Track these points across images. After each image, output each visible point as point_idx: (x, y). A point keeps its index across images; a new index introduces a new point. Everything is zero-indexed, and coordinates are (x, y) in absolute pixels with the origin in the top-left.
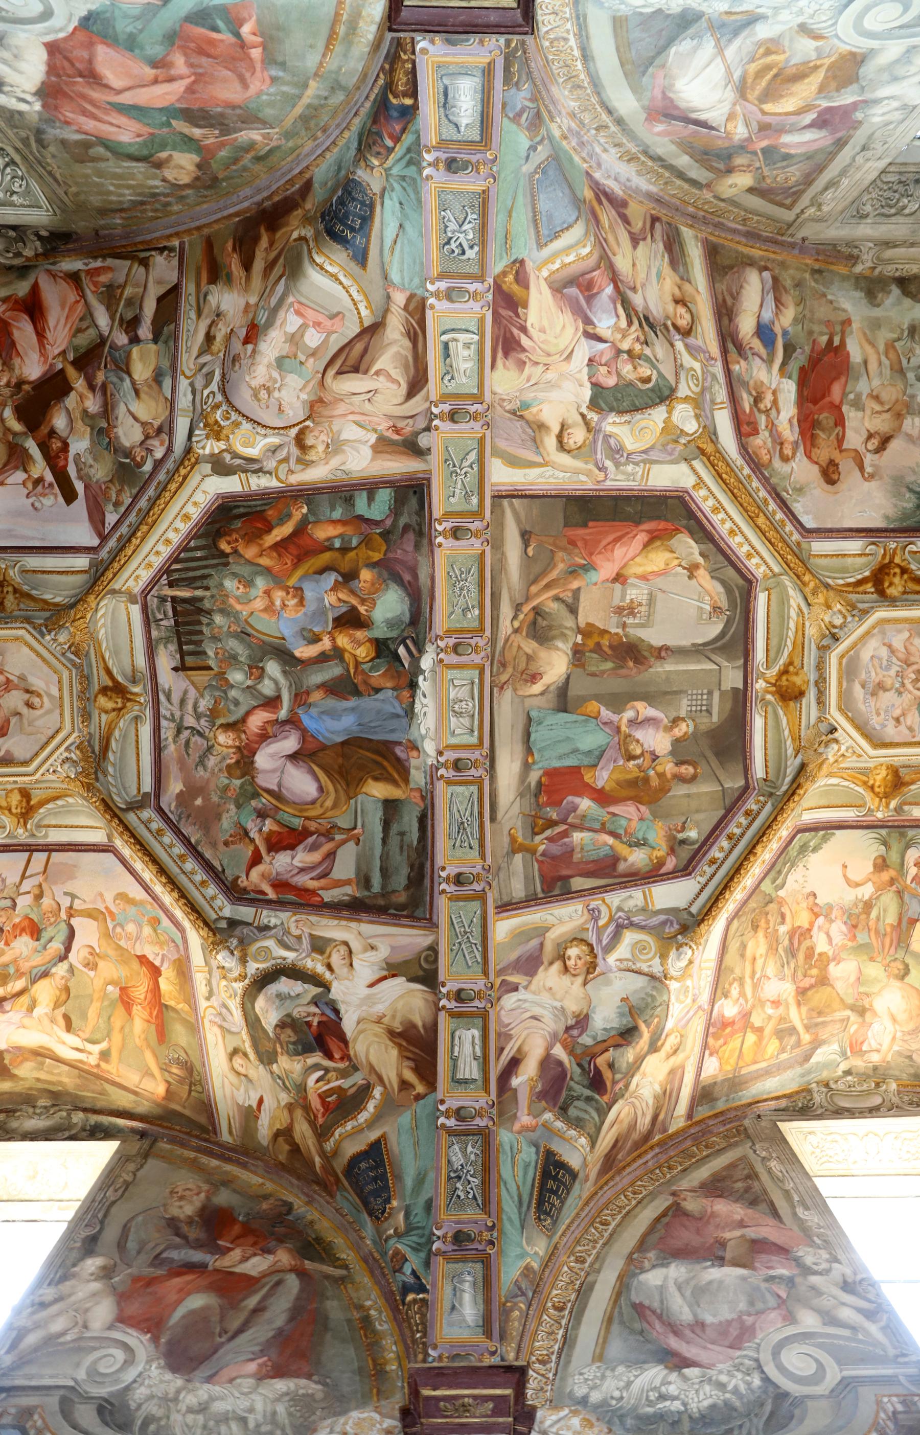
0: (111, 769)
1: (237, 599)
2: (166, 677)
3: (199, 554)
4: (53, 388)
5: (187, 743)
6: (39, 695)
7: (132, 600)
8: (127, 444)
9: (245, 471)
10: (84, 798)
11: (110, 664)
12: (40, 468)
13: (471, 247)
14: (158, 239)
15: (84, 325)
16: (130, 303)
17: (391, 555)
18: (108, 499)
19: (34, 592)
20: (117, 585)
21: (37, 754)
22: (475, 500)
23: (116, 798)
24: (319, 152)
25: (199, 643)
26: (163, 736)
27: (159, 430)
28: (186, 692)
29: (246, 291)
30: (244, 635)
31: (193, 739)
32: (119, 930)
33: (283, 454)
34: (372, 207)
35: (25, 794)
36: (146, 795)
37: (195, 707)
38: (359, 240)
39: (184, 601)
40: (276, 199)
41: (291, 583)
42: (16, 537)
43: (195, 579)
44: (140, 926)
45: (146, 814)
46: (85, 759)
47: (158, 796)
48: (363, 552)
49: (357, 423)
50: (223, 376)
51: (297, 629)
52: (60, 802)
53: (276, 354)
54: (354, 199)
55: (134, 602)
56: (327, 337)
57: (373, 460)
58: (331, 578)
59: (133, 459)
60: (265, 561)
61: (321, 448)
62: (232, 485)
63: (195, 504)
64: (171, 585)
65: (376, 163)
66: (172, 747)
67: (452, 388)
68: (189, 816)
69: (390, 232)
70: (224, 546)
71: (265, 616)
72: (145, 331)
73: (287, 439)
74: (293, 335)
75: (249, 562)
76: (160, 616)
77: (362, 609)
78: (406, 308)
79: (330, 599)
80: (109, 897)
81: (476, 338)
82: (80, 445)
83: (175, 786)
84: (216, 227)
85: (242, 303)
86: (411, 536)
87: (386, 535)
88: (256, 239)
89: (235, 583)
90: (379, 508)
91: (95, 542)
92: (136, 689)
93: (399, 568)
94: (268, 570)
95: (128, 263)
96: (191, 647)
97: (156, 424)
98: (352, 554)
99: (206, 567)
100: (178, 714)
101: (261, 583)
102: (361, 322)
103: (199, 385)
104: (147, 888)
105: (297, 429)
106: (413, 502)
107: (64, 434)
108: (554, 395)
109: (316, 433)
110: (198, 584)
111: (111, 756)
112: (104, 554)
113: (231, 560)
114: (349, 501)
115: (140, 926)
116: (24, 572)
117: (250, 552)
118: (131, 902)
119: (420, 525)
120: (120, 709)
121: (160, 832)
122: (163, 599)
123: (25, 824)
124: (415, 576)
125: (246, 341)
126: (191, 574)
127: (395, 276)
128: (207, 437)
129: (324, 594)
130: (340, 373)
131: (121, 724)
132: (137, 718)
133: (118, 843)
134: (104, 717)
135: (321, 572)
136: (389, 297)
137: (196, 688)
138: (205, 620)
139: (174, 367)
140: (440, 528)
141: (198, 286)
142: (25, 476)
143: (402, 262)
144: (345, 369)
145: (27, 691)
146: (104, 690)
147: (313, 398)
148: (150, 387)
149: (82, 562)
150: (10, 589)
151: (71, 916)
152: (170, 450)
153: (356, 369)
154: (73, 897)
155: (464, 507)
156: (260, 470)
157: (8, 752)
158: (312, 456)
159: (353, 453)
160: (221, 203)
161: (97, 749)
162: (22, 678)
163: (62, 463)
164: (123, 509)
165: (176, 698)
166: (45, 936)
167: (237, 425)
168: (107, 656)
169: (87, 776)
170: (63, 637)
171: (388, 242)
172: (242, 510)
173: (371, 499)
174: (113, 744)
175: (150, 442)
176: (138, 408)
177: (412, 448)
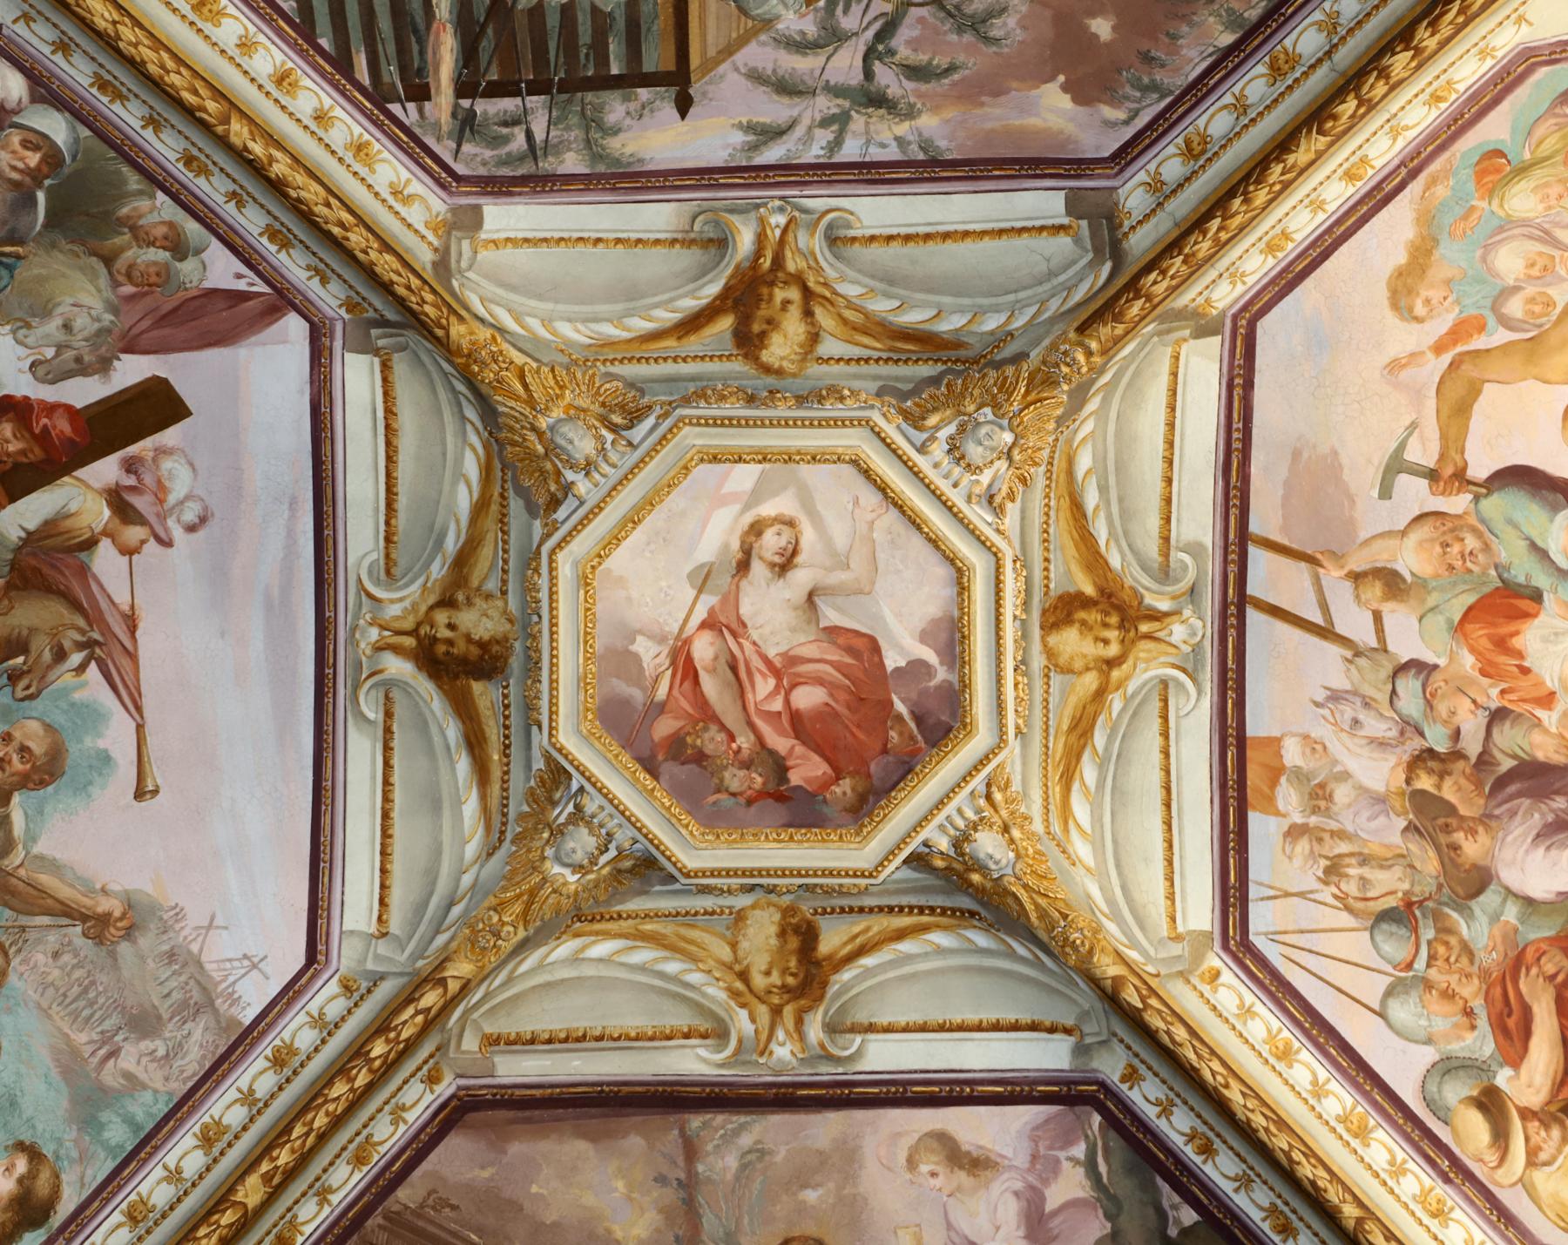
0: (991, 323)
2: (706, 138)
5: (915, 72)
6: (757, 529)
7: (470, 221)
10: (1079, 397)
11: (666, 317)
18: (164, 275)
19: (451, 545)
20: (424, 257)
21: (934, 542)
23: (1079, 295)
26: (892, 153)
28: (756, 77)
31: (904, 53)
32: (1515, 307)
35: (1063, 610)
36: (1074, 206)
37: (801, 46)
39: (468, 54)
42: (287, 588)
44: (1505, 227)
45: (1133, 196)
46: (954, 400)
47: (1079, 166)
52: (1091, 499)
55: (478, 223)
59: (36, 176)
64: (420, 94)
66: (928, 123)
68: (1148, 59)
76: (519, 142)
80: (1405, 338)
83: (1052, 111)
91: (294, 326)
92: (745, 240)
100: (824, 104)
104: (1378, 199)
111: (948, 325)
112: (329, 298)
115: (1505, 227)
116: (389, 571)
118: (1421, 255)
120: (807, 293)
121: (1196, 152)
122: (466, 125)
123: (1156, 616)
126: (384, 23)
131: (851, 290)
132: (833, 240)
133: (1221, 292)
134: (830, 347)
137: (743, 41)
142: (105, 548)
145: (743, 566)
146: (748, 342)
149: (357, 377)
150: (441, 617)
151: (1460, 478)
154: (1397, 465)
157: (924, 637)
161: (926, 370)
162: (703, 579)
164: (192, 227)
165: (774, 110)
166: (1524, 570)
168: (647, 326)
169: (1007, 389)
170: (582, 444)
174: (912, 318)
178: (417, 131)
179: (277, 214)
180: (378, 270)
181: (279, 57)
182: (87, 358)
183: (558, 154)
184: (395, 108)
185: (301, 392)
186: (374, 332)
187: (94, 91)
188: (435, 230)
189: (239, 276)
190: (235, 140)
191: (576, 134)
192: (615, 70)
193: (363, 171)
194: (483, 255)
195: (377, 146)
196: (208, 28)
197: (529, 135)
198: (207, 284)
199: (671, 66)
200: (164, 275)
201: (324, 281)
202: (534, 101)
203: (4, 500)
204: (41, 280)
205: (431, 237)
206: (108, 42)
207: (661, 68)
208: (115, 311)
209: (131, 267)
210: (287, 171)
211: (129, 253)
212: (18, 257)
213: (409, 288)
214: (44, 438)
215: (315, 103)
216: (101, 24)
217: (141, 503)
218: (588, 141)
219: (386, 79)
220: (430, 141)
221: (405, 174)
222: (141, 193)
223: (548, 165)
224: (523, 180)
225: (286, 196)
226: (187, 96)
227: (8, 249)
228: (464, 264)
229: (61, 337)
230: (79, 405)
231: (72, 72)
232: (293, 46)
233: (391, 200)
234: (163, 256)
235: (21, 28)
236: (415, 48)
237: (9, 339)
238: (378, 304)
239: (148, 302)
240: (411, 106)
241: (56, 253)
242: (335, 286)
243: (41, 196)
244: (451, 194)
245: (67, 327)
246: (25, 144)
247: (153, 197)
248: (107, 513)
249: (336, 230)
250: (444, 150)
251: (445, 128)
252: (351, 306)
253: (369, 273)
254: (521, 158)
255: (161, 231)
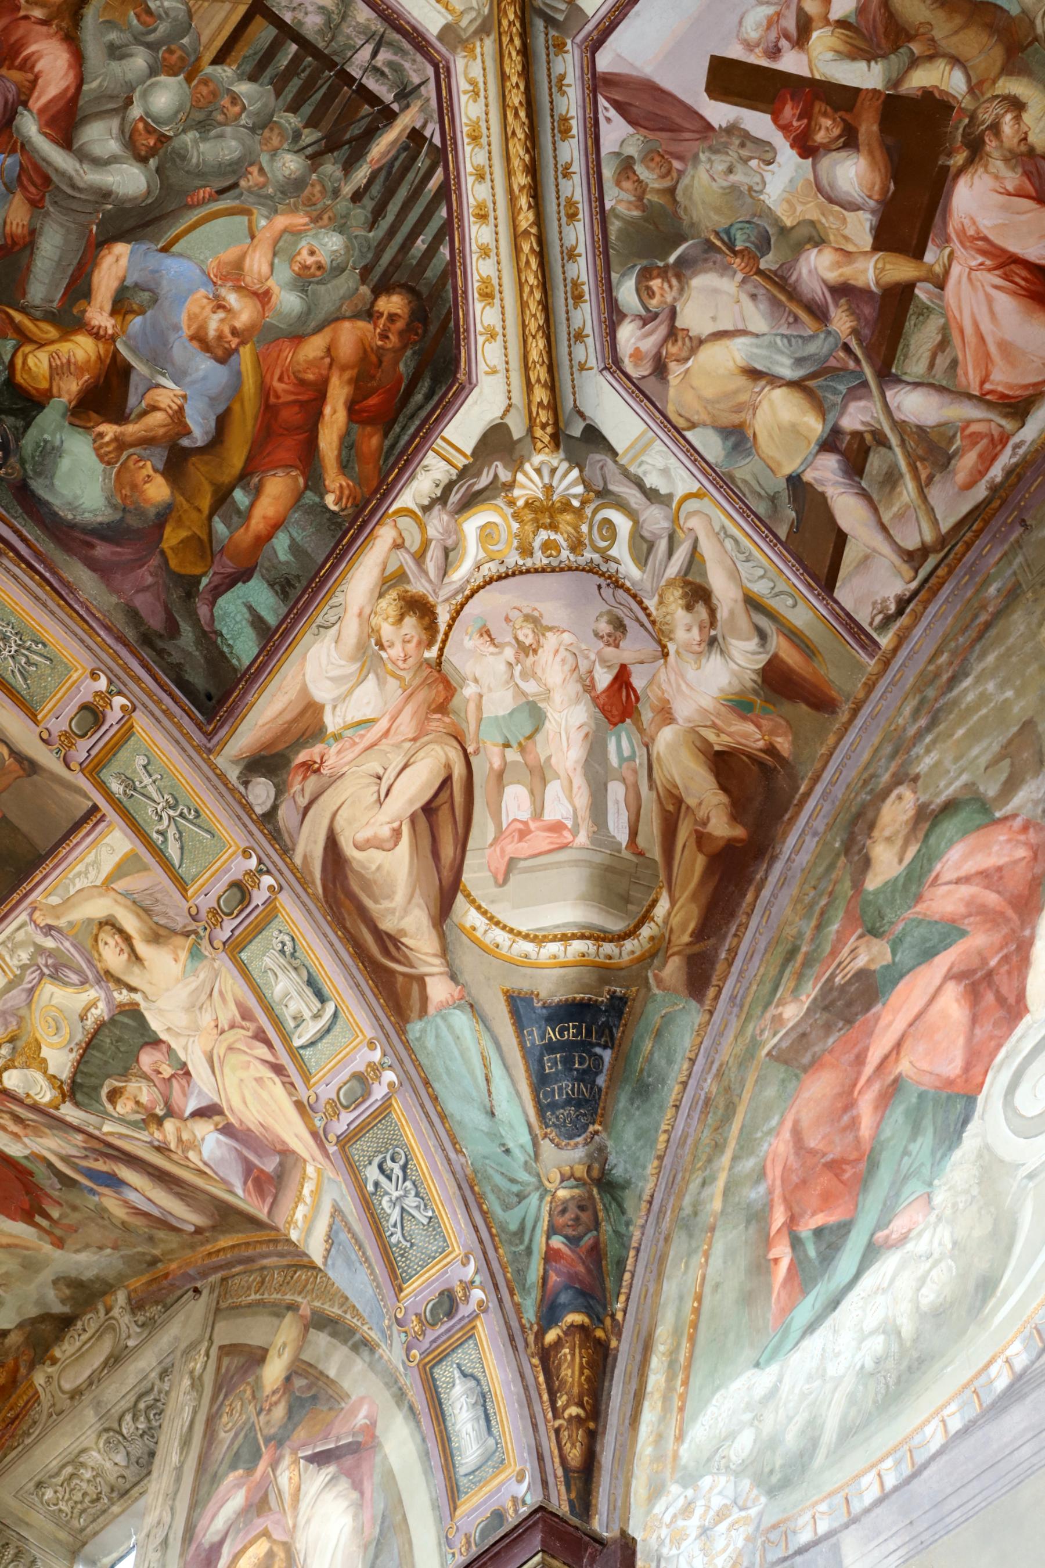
1: (297, 234)
3: (421, 244)
4: (909, 217)
8: (702, 282)
9: (464, 473)
12: (823, 60)
13: (377, 1184)
14: (917, 618)
15: (942, 362)
16: (891, 479)
17: (155, 561)
18: (650, 156)
22: (116, 787)
24: (700, 1061)
25: (279, 85)
27: (660, 369)
29: (693, 731)
30: (228, 182)
33: (432, 563)
34: (541, 1110)
38: (535, 1037)
39: (370, 134)
40: (749, 897)
41: (246, 353)
43: (389, 193)
48: (193, 523)
49: (367, 723)
50: (616, 583)
51: (165, 288)
53: (549, 726)
54: (569, 1102)
55: (447, 31)
56: (498, 824)
57: (304, 690)
58: (199, 431)
59: (663, 273)
60: (314, 348)
61: (387, 631)
62: (464, 427)
63: (493, 336)
64: (416, 136)
65: (562, 1193)
67: (274, 936)
69: (501, 1086)
70: (393, 304)
71: (230, 254)
72: (826, 473)
73: (444, 593)
74: (544, 782)
75: (336, 319)
77: (109, 430)
78: (421, 980)
79: (168, 393)
81: (297, 1042)
82: (782, 181)
84: (831, 739)
85: (684, 710)
86: (156, 622)
87: (189, 586)
88: (737, 811)
89: (324, 257)
90: (237, 615)
91: (605, 62)
93: (126, 553)
94: (298, 338)
95: (945, 527)
96: (283, 60)
97: (675, 370)
98: (205, 503)
99: (392, 232)
101: (288, 301)
102: (468, 896)
103: (655, 519)
105: (442, 627)
106: (198, 679)
107: (826, 162)
108: (182, 993)
109: (411, 647)
110: (376, 190)
112: (569, 65)
113: (365, 290)
114: (283, 586)
117: (349, 336)
119: (160, 653)
124: (92, 565)
125: (622, 678)
126: (402, 193)
127: (461, 1020)
128: (549, 489)
129: (182, 392)
130: (447, 781)
135: (222, 422)
136: (453, 977)
138: (310, 136)
139: (723, 482)
140: (118, 701)
141: (793, 635)
143: (462, 1054)
144: (444, 796)
147: (456, 702)
148: (739, 408)
152: (613, 364)
153: (429, 810)
155: (115, 766)
156: (442, 499)
158: (389, 605)
159: (333, 671)
160: (839, 792)
163: (789, 112)
164: (608, 173)
167: (526, 551)
171: (497, 1071)
172: (418, 397)
173: (257, 621)
175: (662, 331)
176: (737, 352)
177: (269, 762)
178: (436, 116)
179: (550, 146)
180: (519, 68)
181: (474, 229)
182: (737, 142)
183: (367, 27)
184: (437, 141)
185: (638, 14)
186: (561, 17)
187: (587, 297)
188: (473, 50)
189: (608, 120)
190: (531, 216)
191: (347, 30)
192: (294, 47)
193: (483, 125)
194: (460, 8)
195: (465, 129)
196: (495, 282)
197: (375, 54)
198: (630, 130)
199: (259, 20)
200: (650, 156)
201: (562, 77)
202: (356, 73)
203: (862, 95)
204: (718, 210)
205: (478, 50)
206: (548, 331)
207: (265, 23)
208: (696, 158)
209: (663, 177)
210: (519, 174)
211: (656, 185)
212: (717, 234)
213: (512, 40)
214: (806, 114)
215: (477, 186)
216: (541, 343)
217: (790, 24)
218: (344, 18)
219: (428, 162)
220: (434, 103)
221: (464, 98)
222: (617, 217)
223: (378, 26)
224: (399, 29)
225: (533, 160)
226: (534, 266)
227: (718, 243)
228: (473, 14)
229: (739, 168)
230: (767, 117)
231: (588, 317)
232: (461, 226)
233: (482, 93)
234: (640, 169)
235: (592, 362)
236: (397, 164)
237: (768, 190)
238: (541, 38)
239: (675, 148)
240: (427, 133)
241: (695, 219)
242: (558, 68)
243: (672, 259)
244: (447, 62)
245: (730, 170)
246: (651, 294)
247: (613, 209)
248: (815, 35)
249: (522, 114)
250: (430, 91)
251: (419, 103)
252: (560, 47)
253: (527, 72)
254: (390, 44)
255: (627, 185)
